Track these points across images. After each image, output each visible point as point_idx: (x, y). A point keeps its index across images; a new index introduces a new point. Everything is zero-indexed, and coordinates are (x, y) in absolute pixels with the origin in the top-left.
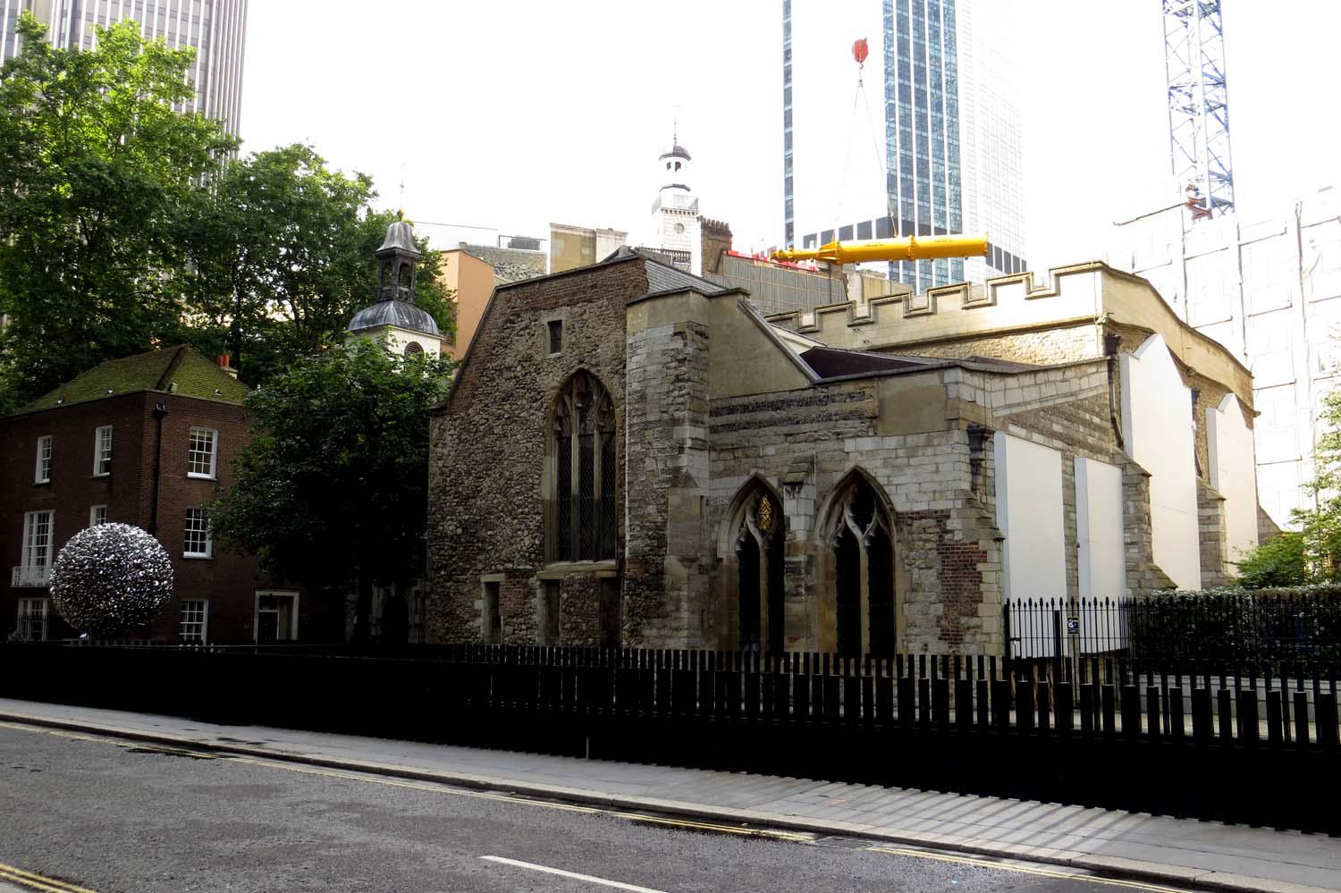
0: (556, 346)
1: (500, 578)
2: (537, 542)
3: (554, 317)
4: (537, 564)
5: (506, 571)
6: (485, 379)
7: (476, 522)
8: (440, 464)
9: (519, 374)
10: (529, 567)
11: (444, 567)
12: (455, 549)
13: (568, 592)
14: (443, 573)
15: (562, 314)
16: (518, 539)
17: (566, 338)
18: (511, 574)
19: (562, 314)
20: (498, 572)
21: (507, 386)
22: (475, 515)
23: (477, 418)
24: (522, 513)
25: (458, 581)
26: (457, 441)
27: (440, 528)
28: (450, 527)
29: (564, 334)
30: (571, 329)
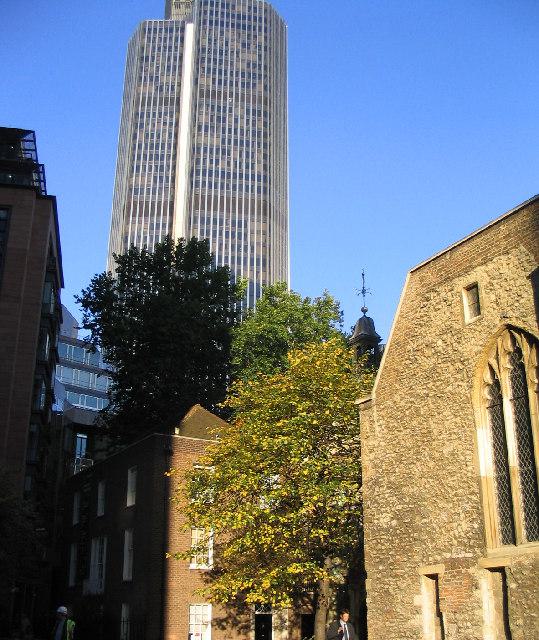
0: (477, 308)
1: (440, 569)
2: (476, 526)
3: (470, 279)
4: (477, 550)
5: (445, 561)
6: (408, 362)
7: (412, 510)
8: (372, 456)
9: (440, 349)
10: (471, 555)
11: (381, 562)
12: (392, 542)
13: (516, 580)
14: (381, 568)
15: (479, 275)
16: (455, 525)
17: (486, 298)
18: (452, 564)
19: (479, 275)
20: (436, 562)
21: (428, 363)
22: (408, 504)
23: (403, 403)
24: (456, 495)
25: (396, 576)
26: (386, 431)
27: (376, 521)
28: (384, 520)
29: (483, 294)
30: (491, 287)
